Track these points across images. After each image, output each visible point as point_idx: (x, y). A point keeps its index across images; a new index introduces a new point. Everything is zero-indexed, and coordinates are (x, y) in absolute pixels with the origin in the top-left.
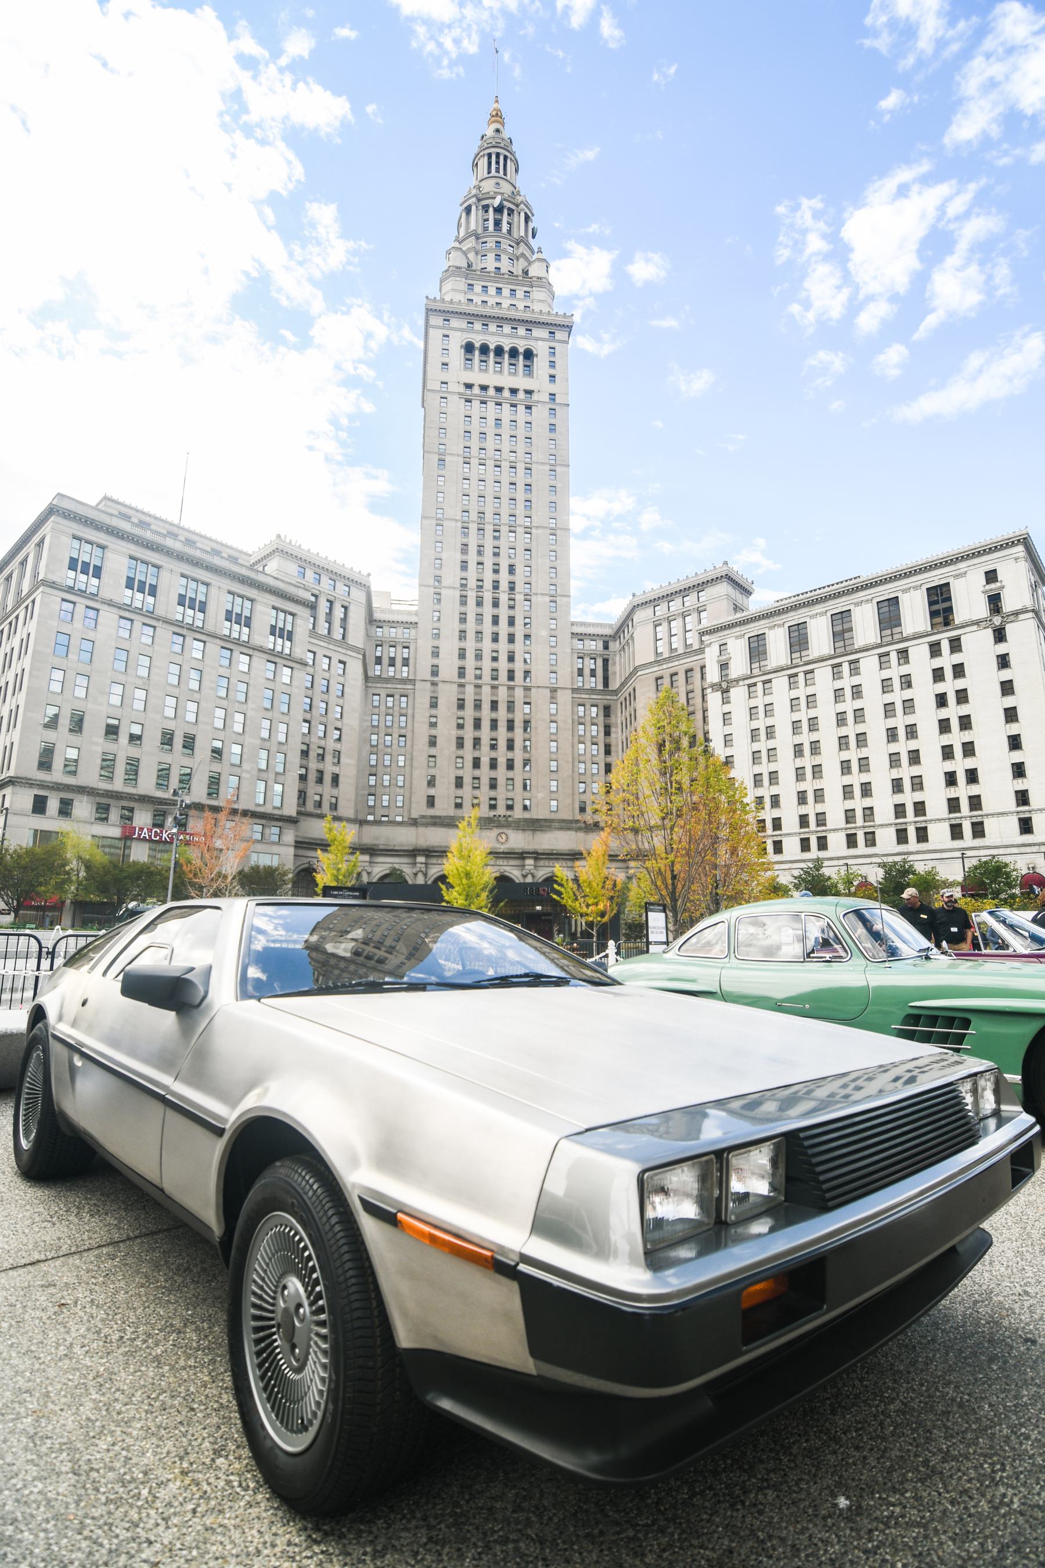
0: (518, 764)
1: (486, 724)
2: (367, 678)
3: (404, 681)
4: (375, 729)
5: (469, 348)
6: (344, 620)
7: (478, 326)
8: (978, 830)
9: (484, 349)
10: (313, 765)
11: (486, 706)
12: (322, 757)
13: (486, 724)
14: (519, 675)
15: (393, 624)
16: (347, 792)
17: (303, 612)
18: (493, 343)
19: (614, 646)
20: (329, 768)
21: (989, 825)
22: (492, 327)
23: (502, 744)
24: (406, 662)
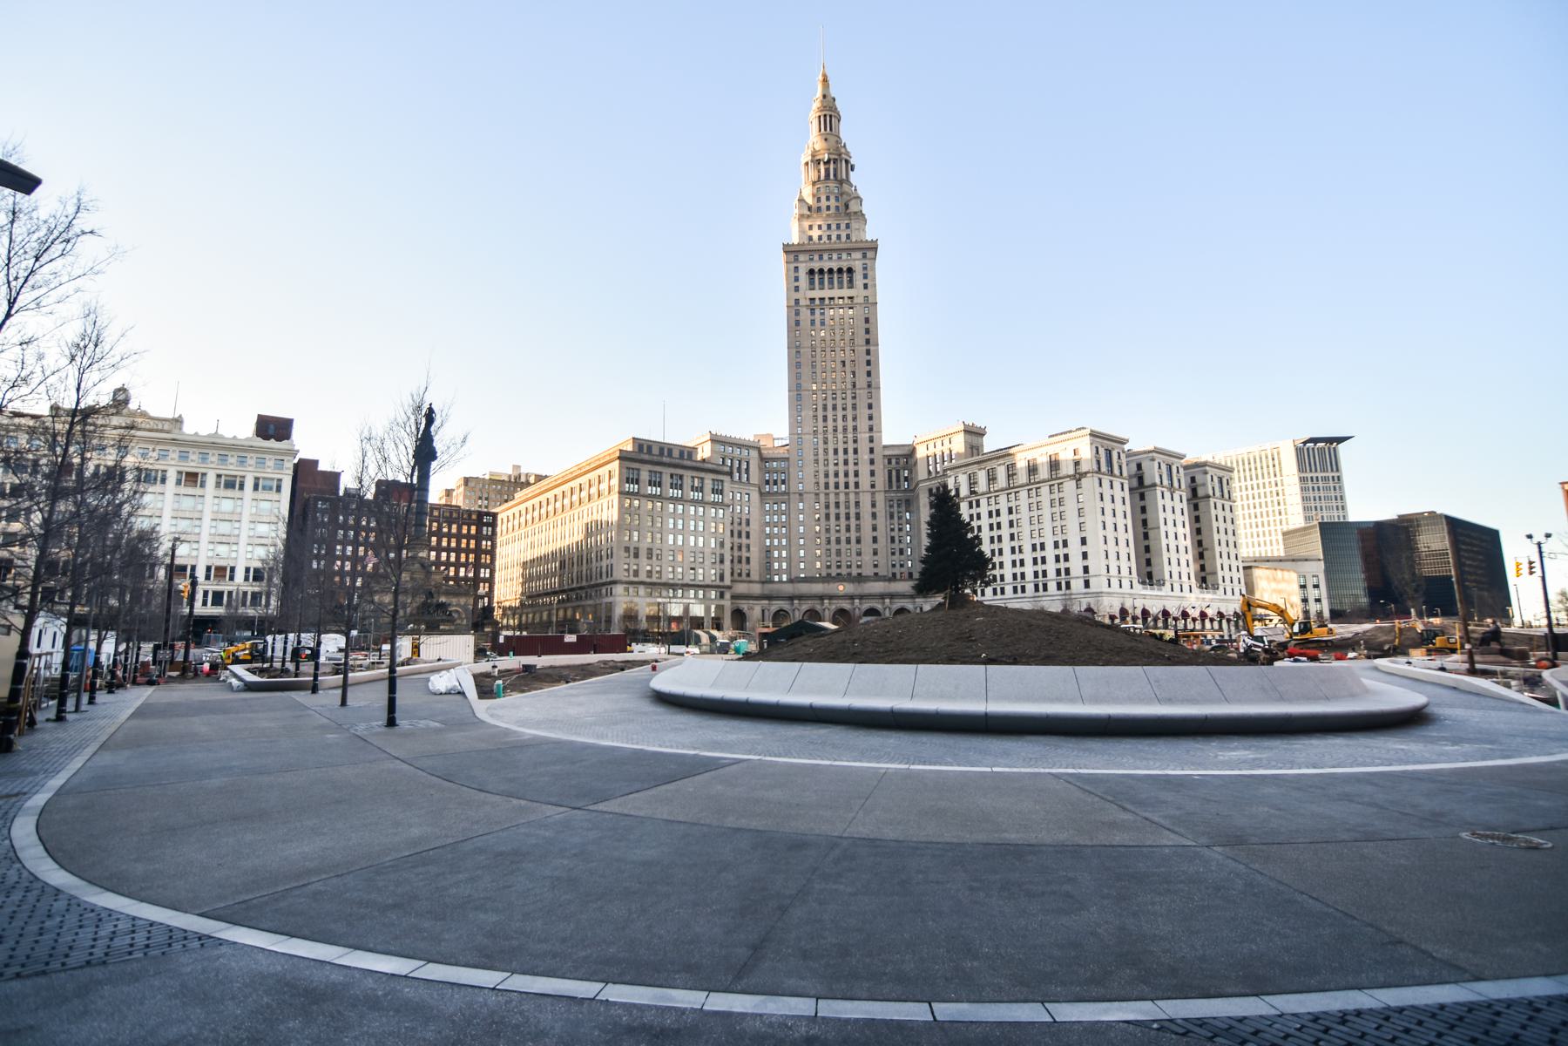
0: (853, 540)
1: (833, 517)
2: (761, 494)
3: (784, 493)
4: (768, 524)
5: (811, 272)
6: (747, 470)
7: (816, 257)
8: (1068, 586)
9: (821, 271)
10: (736, 554)
11: (832, 506)
12: (740, 548)
13: (833, 517)
14: (852, 485)
15: (774, 459)
16: (755, 568)
17: (727, 479)
18: (826, 266)
19: (911, 461)
20: (745, 554)
21: (1073, 583)
22: (826, 257)
23: (843, 528)
24: (783, 482)
